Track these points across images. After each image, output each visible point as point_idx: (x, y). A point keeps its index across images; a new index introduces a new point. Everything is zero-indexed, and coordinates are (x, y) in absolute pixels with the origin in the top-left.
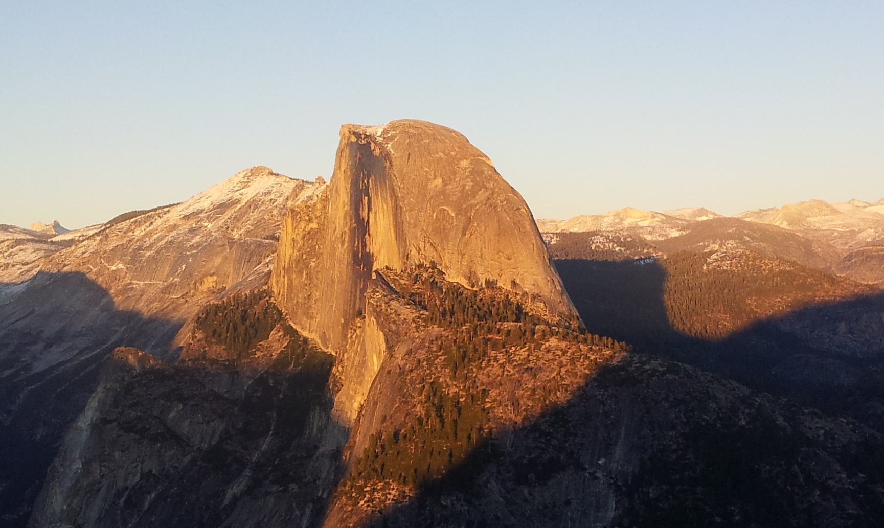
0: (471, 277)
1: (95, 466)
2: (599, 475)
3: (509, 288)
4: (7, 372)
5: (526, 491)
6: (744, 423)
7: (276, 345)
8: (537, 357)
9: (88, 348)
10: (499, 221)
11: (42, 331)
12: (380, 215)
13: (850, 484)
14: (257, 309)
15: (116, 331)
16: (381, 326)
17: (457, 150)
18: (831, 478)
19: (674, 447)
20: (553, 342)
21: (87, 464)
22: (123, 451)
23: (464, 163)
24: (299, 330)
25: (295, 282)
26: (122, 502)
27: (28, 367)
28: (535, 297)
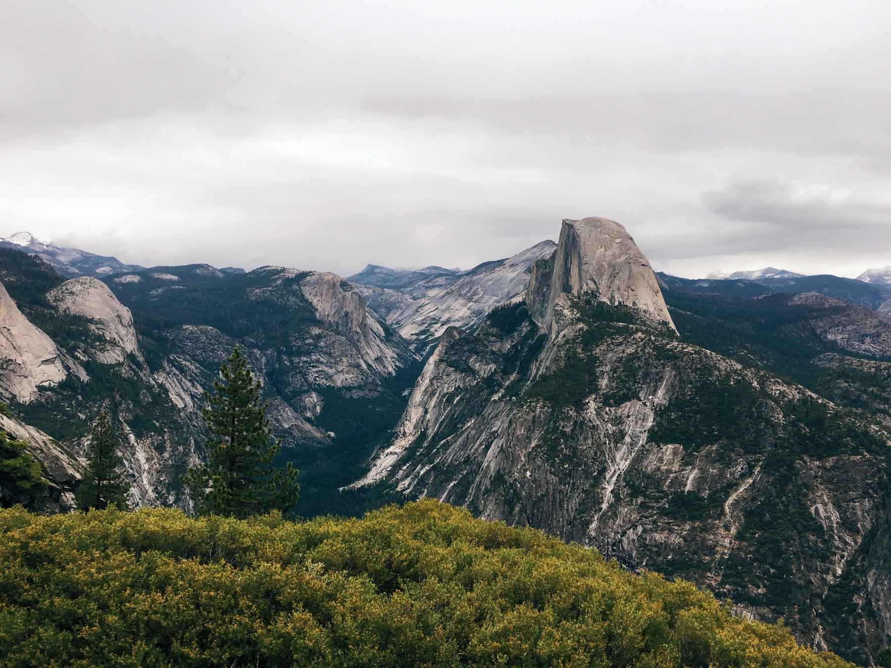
0: (612, 299)
1: (435, 381)
2: (648, 404)
3: (631, 305)
4: (423, 337)
5: (607, 409)
6: (732, 383)
7: (525, 329)
8: (628, 341)
10: (630, 271)
11: (440, 318)
12: (575, 266)
13: (783, 421)
14: (518, 311)
15: (473, 320)
16: (557, 322)
17: (616, 233)
18: (772, 417)
19: (689, 393)
20: (640, 334)
21: (431, 380)
22: (447, 375)
23: (618, 241)
24: (536, 322)
25: (537, 298)
26: (444, 400)
27: (432, 335)
28: (645, 311)
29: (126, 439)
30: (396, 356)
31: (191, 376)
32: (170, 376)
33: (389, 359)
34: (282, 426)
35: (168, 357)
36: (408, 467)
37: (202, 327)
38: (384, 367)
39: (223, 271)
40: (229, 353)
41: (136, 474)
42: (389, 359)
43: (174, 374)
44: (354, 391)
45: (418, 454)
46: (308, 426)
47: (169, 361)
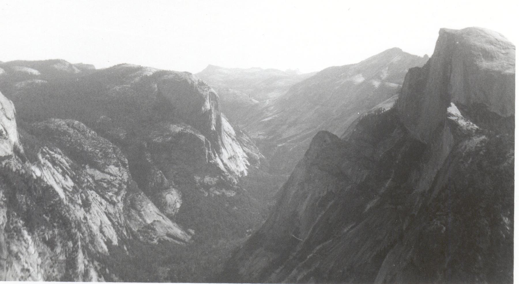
9: (307, 129)
26: (317, 203)
29: (18, 232)
30: (246, 156)
31: (62, 168)
32: (45, 168)
33: (241, 158)
34: (145, 221)
35: (42, 150)
36: (281, 271)
37: (68, 121)
38: (237, 166)
39: (80, 66)
40: (95, 147)
41: (31, 268)
42: (241, 158)
43: (48, 167)
44: (211, 189)
45: (291, 257)
46: (168, 223)
47: (43, 154)
